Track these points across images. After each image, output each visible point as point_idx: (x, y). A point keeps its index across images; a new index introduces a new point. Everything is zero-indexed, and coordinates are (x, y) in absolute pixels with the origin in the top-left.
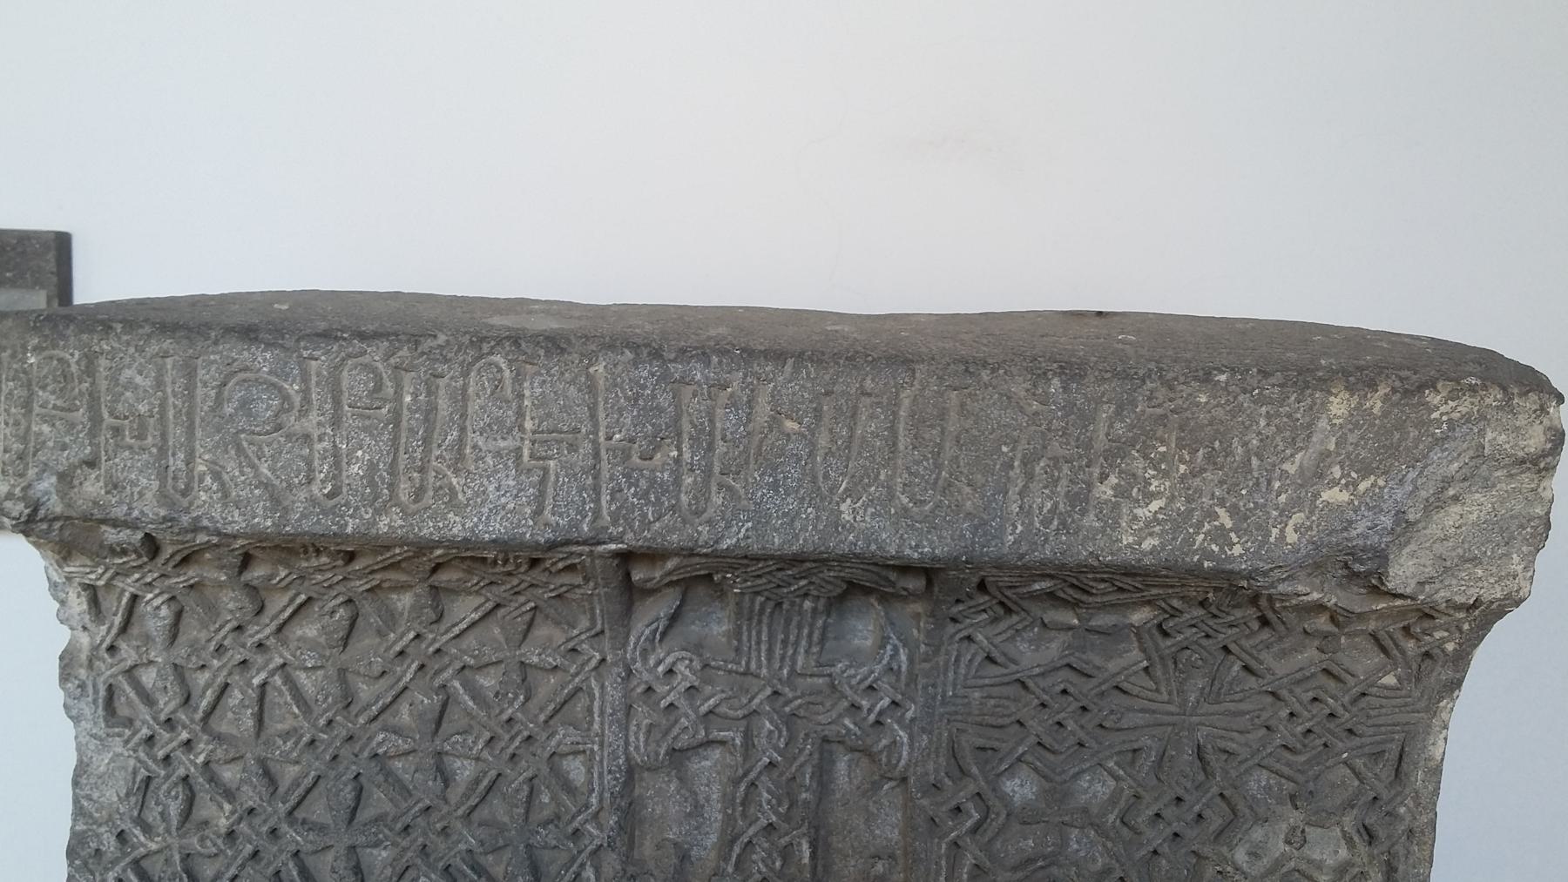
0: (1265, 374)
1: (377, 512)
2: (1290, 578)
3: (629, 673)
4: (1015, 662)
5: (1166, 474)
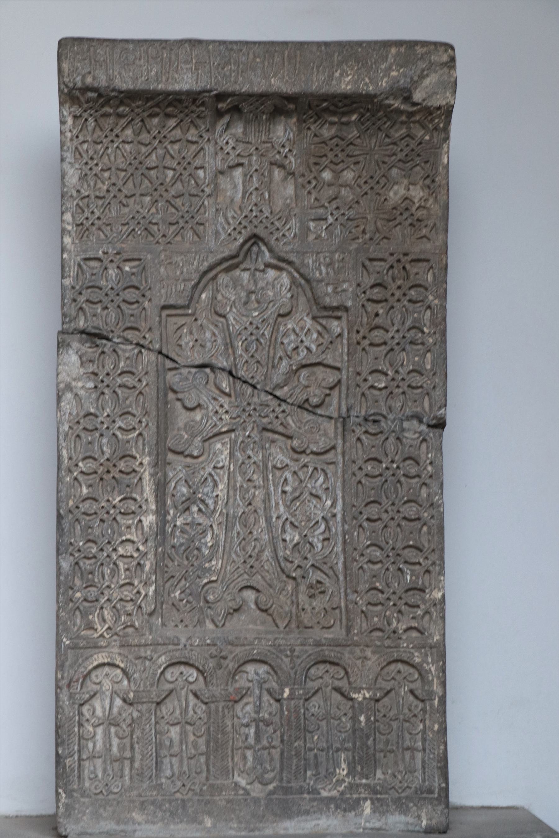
1: (158, 84)
2: (387, 98)
3: (216, 143)
5: (352, 70)
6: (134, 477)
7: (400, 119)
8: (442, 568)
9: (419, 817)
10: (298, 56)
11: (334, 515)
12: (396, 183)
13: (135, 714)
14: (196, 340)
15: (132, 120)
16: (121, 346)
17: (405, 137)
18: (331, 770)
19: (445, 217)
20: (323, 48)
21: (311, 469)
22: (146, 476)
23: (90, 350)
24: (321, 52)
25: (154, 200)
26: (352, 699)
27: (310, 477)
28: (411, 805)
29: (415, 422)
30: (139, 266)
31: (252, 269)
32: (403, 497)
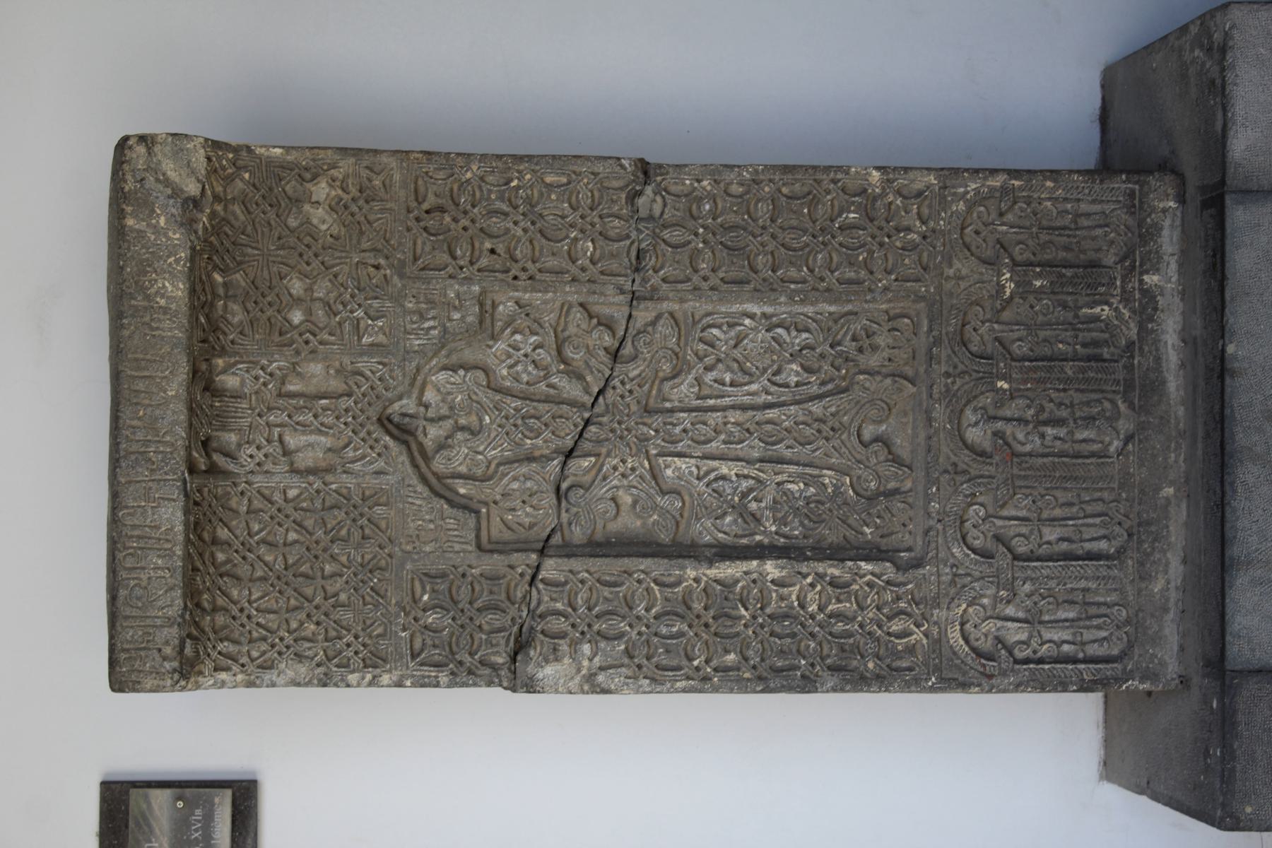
0: (120, 248)
1: (174, 552)
2: (196, 232)
3: (252, 472)
4: (242, 322)
6: (714, 589)
7: (222, 213)
8: (839, 169)
9: (1164, 211)
10: (136, 356)
11: (764, 315)
12: (308, 222)
13: (1028, 587)
14: (524, 502)
15: (219, 589)
16: (532, 606)
17: (245, 206)
18: (1102, 325)
19: (357, 152)
20: (126, 321)
21: (701, 346)
22: (712, 572)
23: (538, 648)
24: (130, 324)
25: (331, 560)
26: (1011, 297)
27: (713, 346)
28: (1149, 220)
29: (641, 201)
30: (421, 580)
31: (425, 423)
32: (744, 220)
